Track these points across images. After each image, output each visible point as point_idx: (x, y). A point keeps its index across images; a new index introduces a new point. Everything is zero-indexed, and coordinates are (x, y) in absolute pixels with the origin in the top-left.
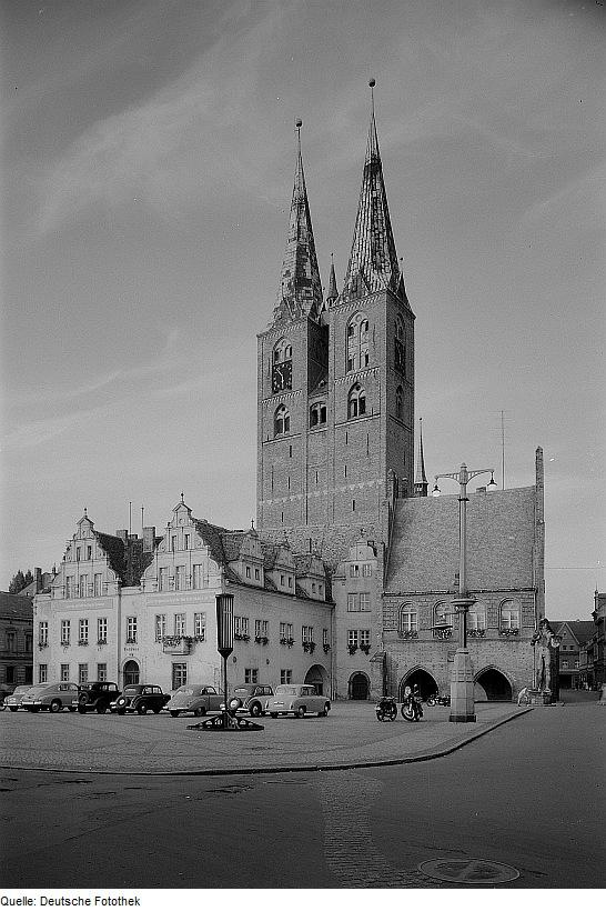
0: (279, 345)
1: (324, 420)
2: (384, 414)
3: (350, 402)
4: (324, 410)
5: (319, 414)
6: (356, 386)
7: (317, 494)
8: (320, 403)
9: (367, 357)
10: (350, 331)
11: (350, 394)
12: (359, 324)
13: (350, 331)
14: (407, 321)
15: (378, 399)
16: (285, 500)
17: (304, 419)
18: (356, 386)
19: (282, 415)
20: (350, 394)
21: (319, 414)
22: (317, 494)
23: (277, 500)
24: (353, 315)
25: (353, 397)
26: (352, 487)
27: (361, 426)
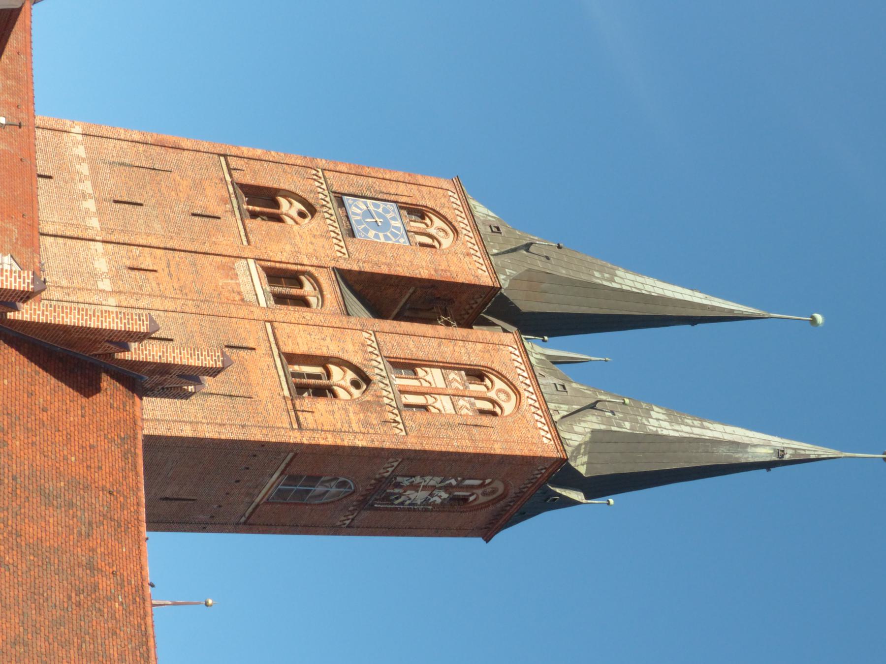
1: (280, 299)
2: (295, 437)
3: (324, 361)
4: (303, 302)
5: (295, 291)
6: (362, 379)
7: (101, 265)
9: (425, 408)
10: (477, 374)
11: (343, 363)
12: (492, 394)
13: (477, 374)
14: (482, 516)
15: (337, 422)
16: (87, 186)
17: (282, 254)
18: (362, 379)
19: (289, 208)
20: (343, 363)
21: (295, 291)
22: (101, 265)
23: (84, 169)
27: (268, 380)
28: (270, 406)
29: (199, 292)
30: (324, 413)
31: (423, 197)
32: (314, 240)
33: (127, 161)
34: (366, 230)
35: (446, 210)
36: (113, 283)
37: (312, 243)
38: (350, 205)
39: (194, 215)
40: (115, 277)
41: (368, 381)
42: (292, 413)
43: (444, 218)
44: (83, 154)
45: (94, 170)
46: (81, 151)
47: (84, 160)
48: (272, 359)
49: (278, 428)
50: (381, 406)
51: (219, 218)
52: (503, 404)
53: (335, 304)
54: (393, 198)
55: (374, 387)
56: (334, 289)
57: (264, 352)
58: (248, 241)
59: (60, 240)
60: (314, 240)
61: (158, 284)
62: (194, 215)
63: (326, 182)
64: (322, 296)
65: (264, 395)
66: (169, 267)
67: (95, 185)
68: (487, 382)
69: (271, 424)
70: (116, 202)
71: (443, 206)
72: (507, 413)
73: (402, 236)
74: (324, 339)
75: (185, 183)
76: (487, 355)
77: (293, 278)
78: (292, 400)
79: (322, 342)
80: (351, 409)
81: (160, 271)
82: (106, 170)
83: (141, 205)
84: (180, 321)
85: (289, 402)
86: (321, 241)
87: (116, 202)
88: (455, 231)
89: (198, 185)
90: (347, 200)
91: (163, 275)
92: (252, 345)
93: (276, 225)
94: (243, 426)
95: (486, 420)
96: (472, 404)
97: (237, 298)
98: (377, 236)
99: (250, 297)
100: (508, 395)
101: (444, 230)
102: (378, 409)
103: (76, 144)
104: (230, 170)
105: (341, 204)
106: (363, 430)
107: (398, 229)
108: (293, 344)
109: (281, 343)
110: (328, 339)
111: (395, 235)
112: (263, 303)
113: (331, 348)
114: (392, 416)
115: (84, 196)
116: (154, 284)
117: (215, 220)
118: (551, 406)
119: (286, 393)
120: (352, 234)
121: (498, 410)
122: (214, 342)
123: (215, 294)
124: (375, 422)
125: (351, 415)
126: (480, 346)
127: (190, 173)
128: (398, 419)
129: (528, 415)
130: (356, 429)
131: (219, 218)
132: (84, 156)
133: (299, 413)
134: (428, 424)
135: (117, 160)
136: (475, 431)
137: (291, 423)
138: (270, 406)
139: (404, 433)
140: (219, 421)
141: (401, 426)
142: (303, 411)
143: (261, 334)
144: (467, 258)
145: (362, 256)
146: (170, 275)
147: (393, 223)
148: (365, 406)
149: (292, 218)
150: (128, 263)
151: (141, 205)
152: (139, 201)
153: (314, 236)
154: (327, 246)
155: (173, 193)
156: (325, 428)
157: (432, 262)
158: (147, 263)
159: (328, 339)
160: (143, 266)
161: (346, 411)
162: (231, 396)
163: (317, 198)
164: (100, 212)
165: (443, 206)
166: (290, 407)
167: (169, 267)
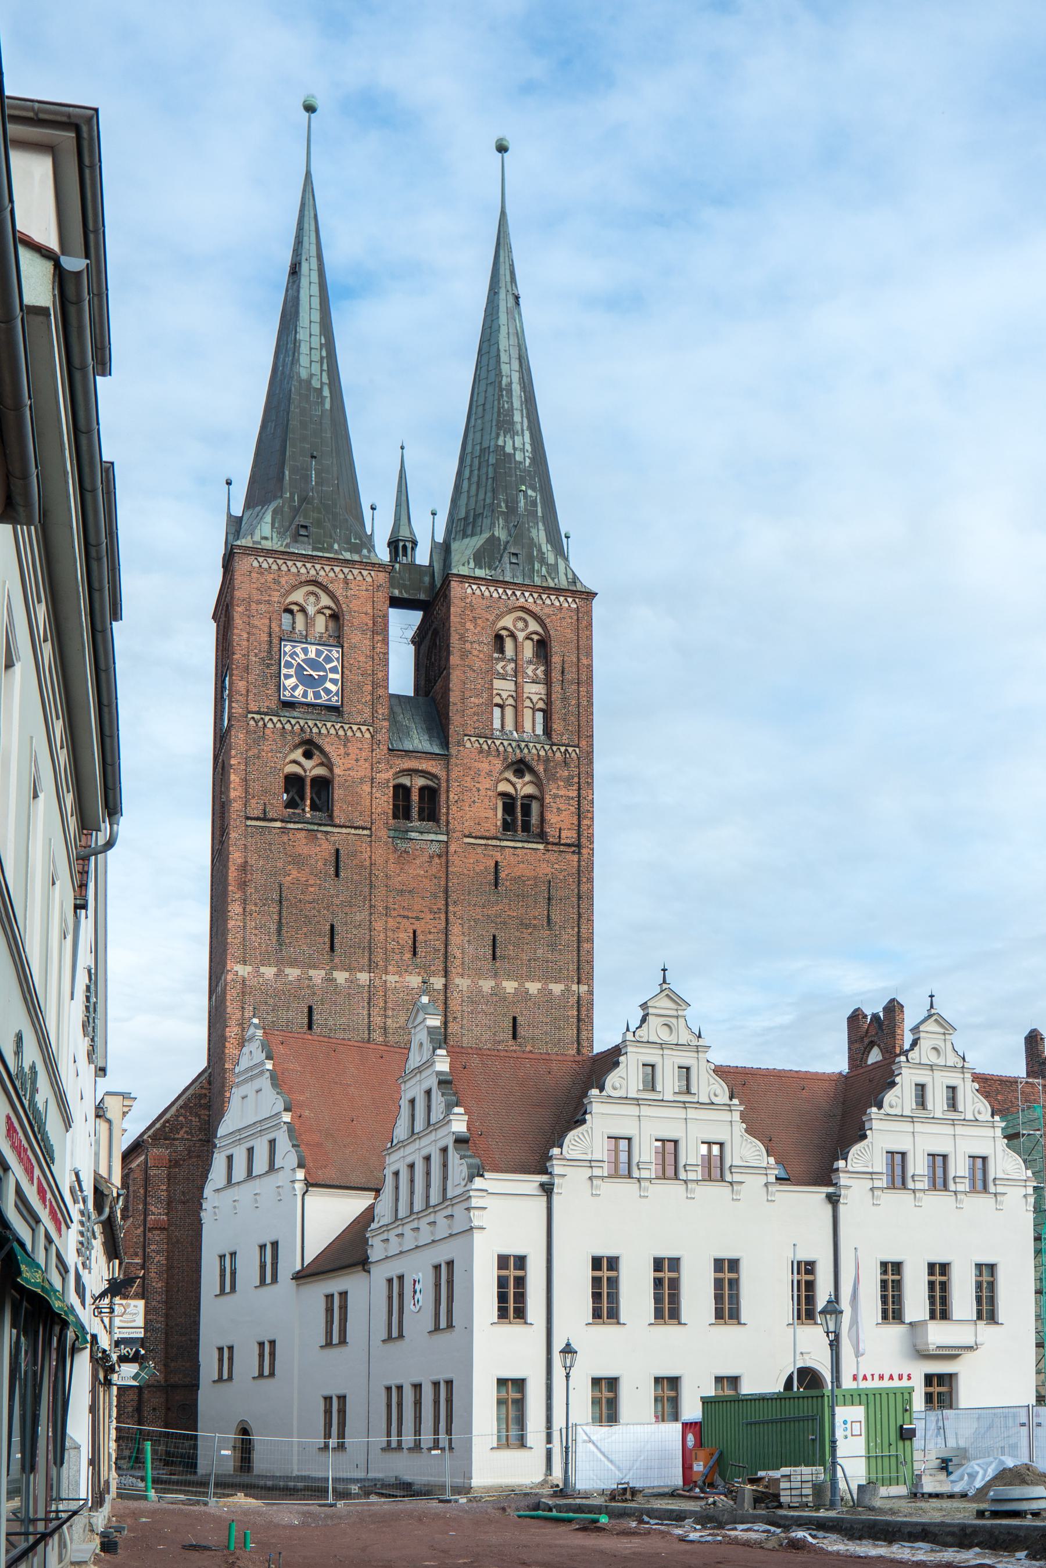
0: (298, 596)
5: (415, 797)
6: (521, 767)
8: (424, 774)
16: (317, 975)
19: (312, 769)
21: (415, 797)
23: (293, 973)
24: (511, 611)
25: (503, 787)
26: (510, 986)
28: (556, 866)
29: (435, 896)
30: (559, 819)
31: (268, 602)
32: (353, 756)
33: (273, 927)
34: (328, 691)
35: (283, 581)
36: (434, 974)
37: (357, 760)
38: (292, 696)
39: (337, 875)
40: (426, 970)
41: (521, 761)
42: (562, 848)
43: (295, 588)
44: (273, 970)
45: (293, 964)
46: (269, 972)
47: (279, 970)
48: (507, 850)
49: (579, 866)
50: (547, 760)
51: (337, 850)
52: (531, 629)
53: (434, 763)
54: (275, 641)
55: (528, 758)
56: (416, 757)
57: (499, 854)
58: (364, 828)
59: (390, 1013)
60: (353, 756)
61: (430, 933)
62: (337, 875)
63: (266, 714)
64: (422, 771)
65: (544, 869)
66: (408, 918)
67: (315, 967)
68: (504, 633)
69: (574, 871)
70: (332, 949)
71: (276, 582)
72: (540, 630)
73: (330, 651)
74: (479, 790)
75: (294, 873)
76: (479, 621)
77: (401, 793)
78: (548, 843)
79: (483, 792)
80: (554, 791)
81: (414, 927)
82: (290, 952)
83: (332, 926)
84: (472, 923)
85: (550, 847)
86: (353, 749)
87: (332, 949)
88: (315, 582)
89: (298, 861)
90: (286, 695)
91: (418, 926)
92: (493, 865)
93: (338, 793)
94: (579, 898)
95: (556, 659)
96: (530, 662)
97: (436, 860)
98: (334, 681)
99: (435, 848)
100: (520, 618)
101: (313, 593)
102: (552, 764)
103: (258, 974)
104: (264, 819)
105: (289, 705)
106: (575, 787)
107: (319, 653)
108: (487, 822)
109: (487, 834)
110: (477, 785)
111: (328, 659)
112: (444, 838)
113: (488, 786)
114: (558, 754)
115: (330, 980)
116: (431, 937)
117: (342, 857)
118: (537, 581)
119: (541, 847)
120: (336, 710)
121: (536, 637)
122: (493, 899)
123: (435, 881)
124: (566, 773)
125: (561, 793)
126: (469, 625)
127: (280, 865)
128: (563, 749)
129: (546, 610)
130: (575, 794)
131: (337, 850)
132: (275, 969)
133: (562, 842)
134: (564, 720)
135: (274, 938)
136: (568, 676)
137: (574, 852)
138: (556, 866)
139: (577, 750)
140: (575, 917)
141: (570, 749)
142: (559, 837)
143: (479, 850)
144: (352, 586)
145: (367, 710)
146: (418, 919)
147: (312, 655)
148: (552, 777)
149: (314, 767)
150: (408, 955)
151: (332, 926)
152: (328, 927)
153: (348, 755)
154: (359, 745)
155: (311, 889)
156: (576, 823)
157: (364, 632)
158: (405, 937)
159: (477, 785)
160: (410, 942)
161: (556, 796)
162: (549, 899)
163: (292, 732)
164: (349, 969)
165: (276, 582)
166: (555, 848)
167: (408, 918)
